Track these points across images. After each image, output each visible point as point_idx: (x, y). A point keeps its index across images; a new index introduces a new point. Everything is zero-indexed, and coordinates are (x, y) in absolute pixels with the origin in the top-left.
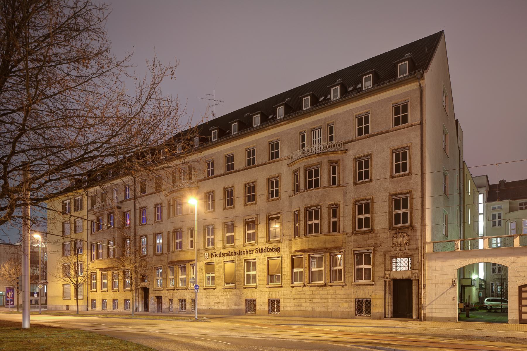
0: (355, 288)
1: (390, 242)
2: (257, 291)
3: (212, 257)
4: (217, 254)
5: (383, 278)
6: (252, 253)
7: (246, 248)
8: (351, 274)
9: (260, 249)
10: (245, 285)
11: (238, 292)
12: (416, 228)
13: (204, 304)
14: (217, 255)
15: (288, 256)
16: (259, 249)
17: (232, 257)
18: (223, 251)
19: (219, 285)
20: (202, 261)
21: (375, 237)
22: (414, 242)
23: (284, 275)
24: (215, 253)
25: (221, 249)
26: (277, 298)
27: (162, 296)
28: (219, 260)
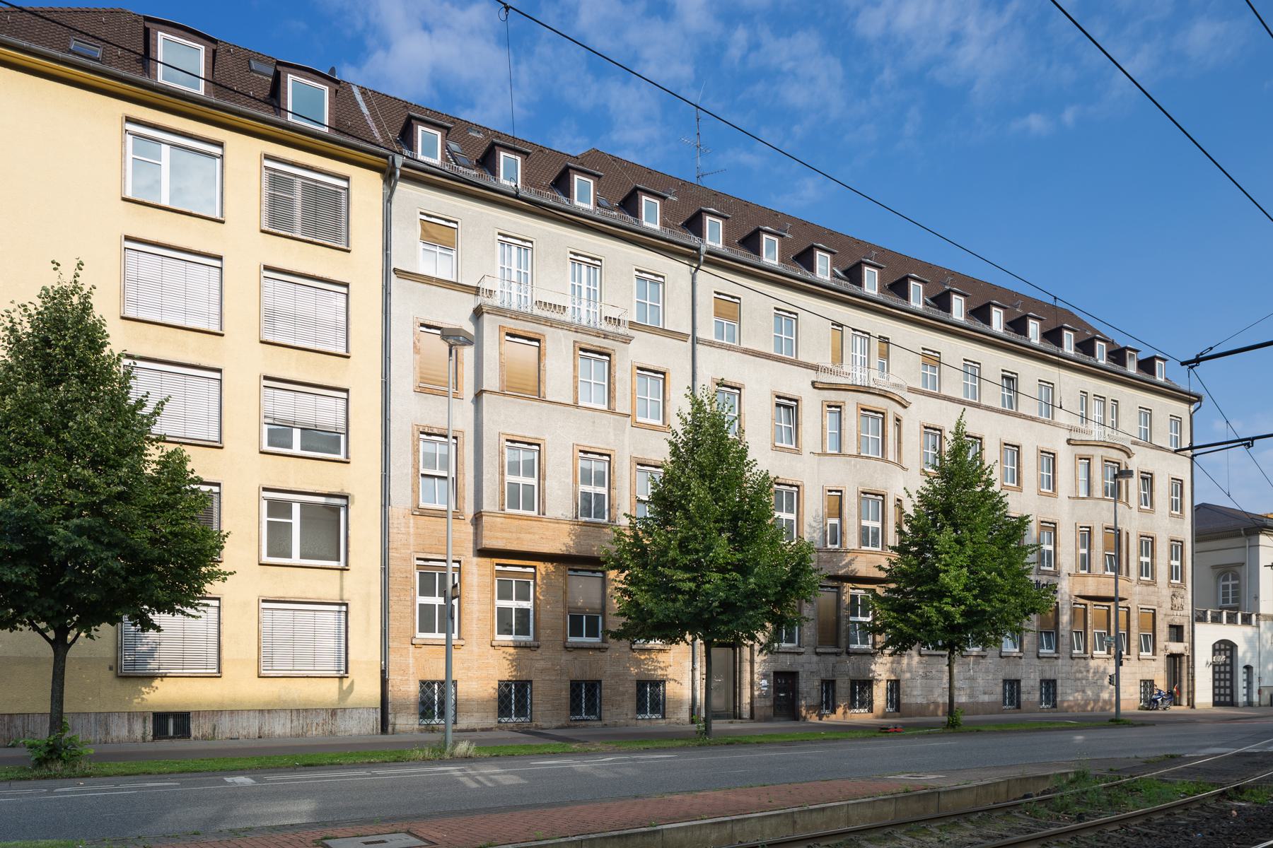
2: (1023, 663)
11: (990, 666)
13: (919, 693)
26: (1052, 678)
27: (800, 670)
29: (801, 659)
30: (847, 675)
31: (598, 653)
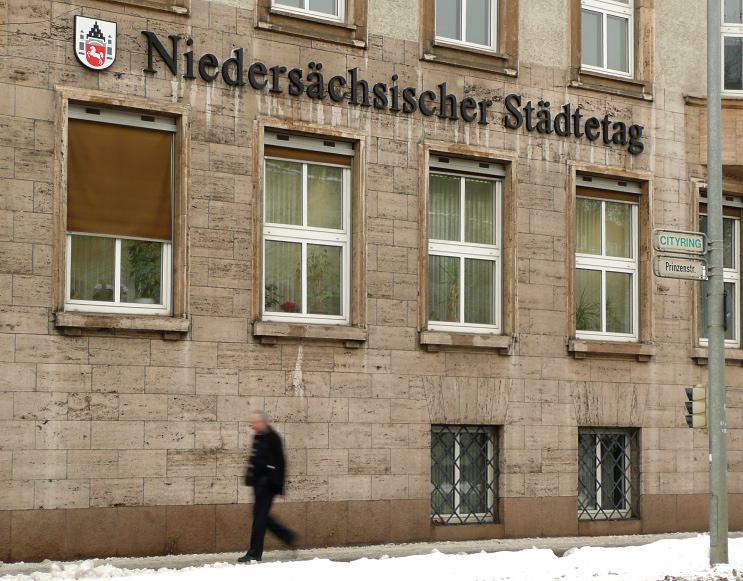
4: (210, 61)
6: (483, 123)
9: (534, 104)
11: (378, 376)
13: (51, 471)
14: (204, 69)
15: (683, 185)
17: (336, 110)
18: (259, 50)
19: (215, 309)
20: (35, 80)
23: (661, 289)
24: (182, 50)
25: (245, 28)
26: (625, 422)
28: (217, 110)
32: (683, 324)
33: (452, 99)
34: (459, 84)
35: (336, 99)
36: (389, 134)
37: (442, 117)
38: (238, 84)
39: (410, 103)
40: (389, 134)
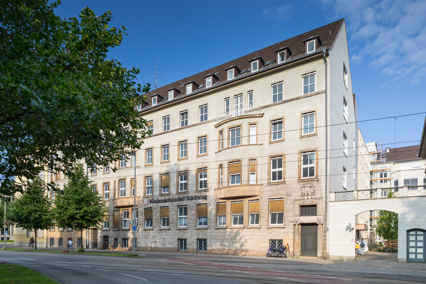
0: (270, 230)
1: (299, 192)
3: (150, 203)
4: (155, 201)
5: (293, 222)
6: (184, 200)
7: (179, 196)
8: (266, 219)
9: (191, 197)
10: (178, 227)
11: (172, 233)
12: (321, 180)
16: (190, 197)
17: (167, 203)
18: (160, 198)
19: (156, 227)
21: (287, 187)
22: (319, 192)
23: (210, 219)
24: (153, 200)
25: (158, 196)
26: (204, 238)
27: (109, 235)
28: (156, 206)
29: (110, 232)
30: (121, 237)
31: (71, 232)
32: (214, 224)
33: (180, 198)
34: (181, 196)
35: (167, 202)
36: (173, 204)
37: (179, 201)
38: (158, 203)
39: (175, 200)
40: (173, 204)
